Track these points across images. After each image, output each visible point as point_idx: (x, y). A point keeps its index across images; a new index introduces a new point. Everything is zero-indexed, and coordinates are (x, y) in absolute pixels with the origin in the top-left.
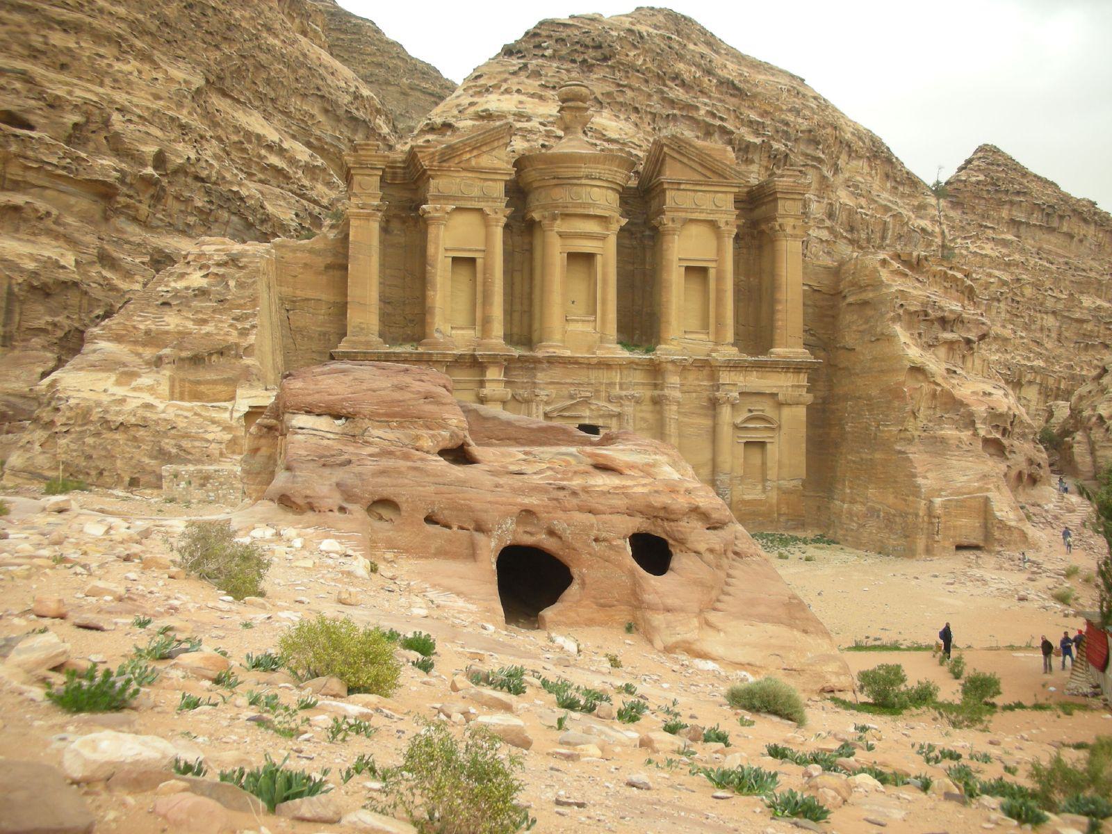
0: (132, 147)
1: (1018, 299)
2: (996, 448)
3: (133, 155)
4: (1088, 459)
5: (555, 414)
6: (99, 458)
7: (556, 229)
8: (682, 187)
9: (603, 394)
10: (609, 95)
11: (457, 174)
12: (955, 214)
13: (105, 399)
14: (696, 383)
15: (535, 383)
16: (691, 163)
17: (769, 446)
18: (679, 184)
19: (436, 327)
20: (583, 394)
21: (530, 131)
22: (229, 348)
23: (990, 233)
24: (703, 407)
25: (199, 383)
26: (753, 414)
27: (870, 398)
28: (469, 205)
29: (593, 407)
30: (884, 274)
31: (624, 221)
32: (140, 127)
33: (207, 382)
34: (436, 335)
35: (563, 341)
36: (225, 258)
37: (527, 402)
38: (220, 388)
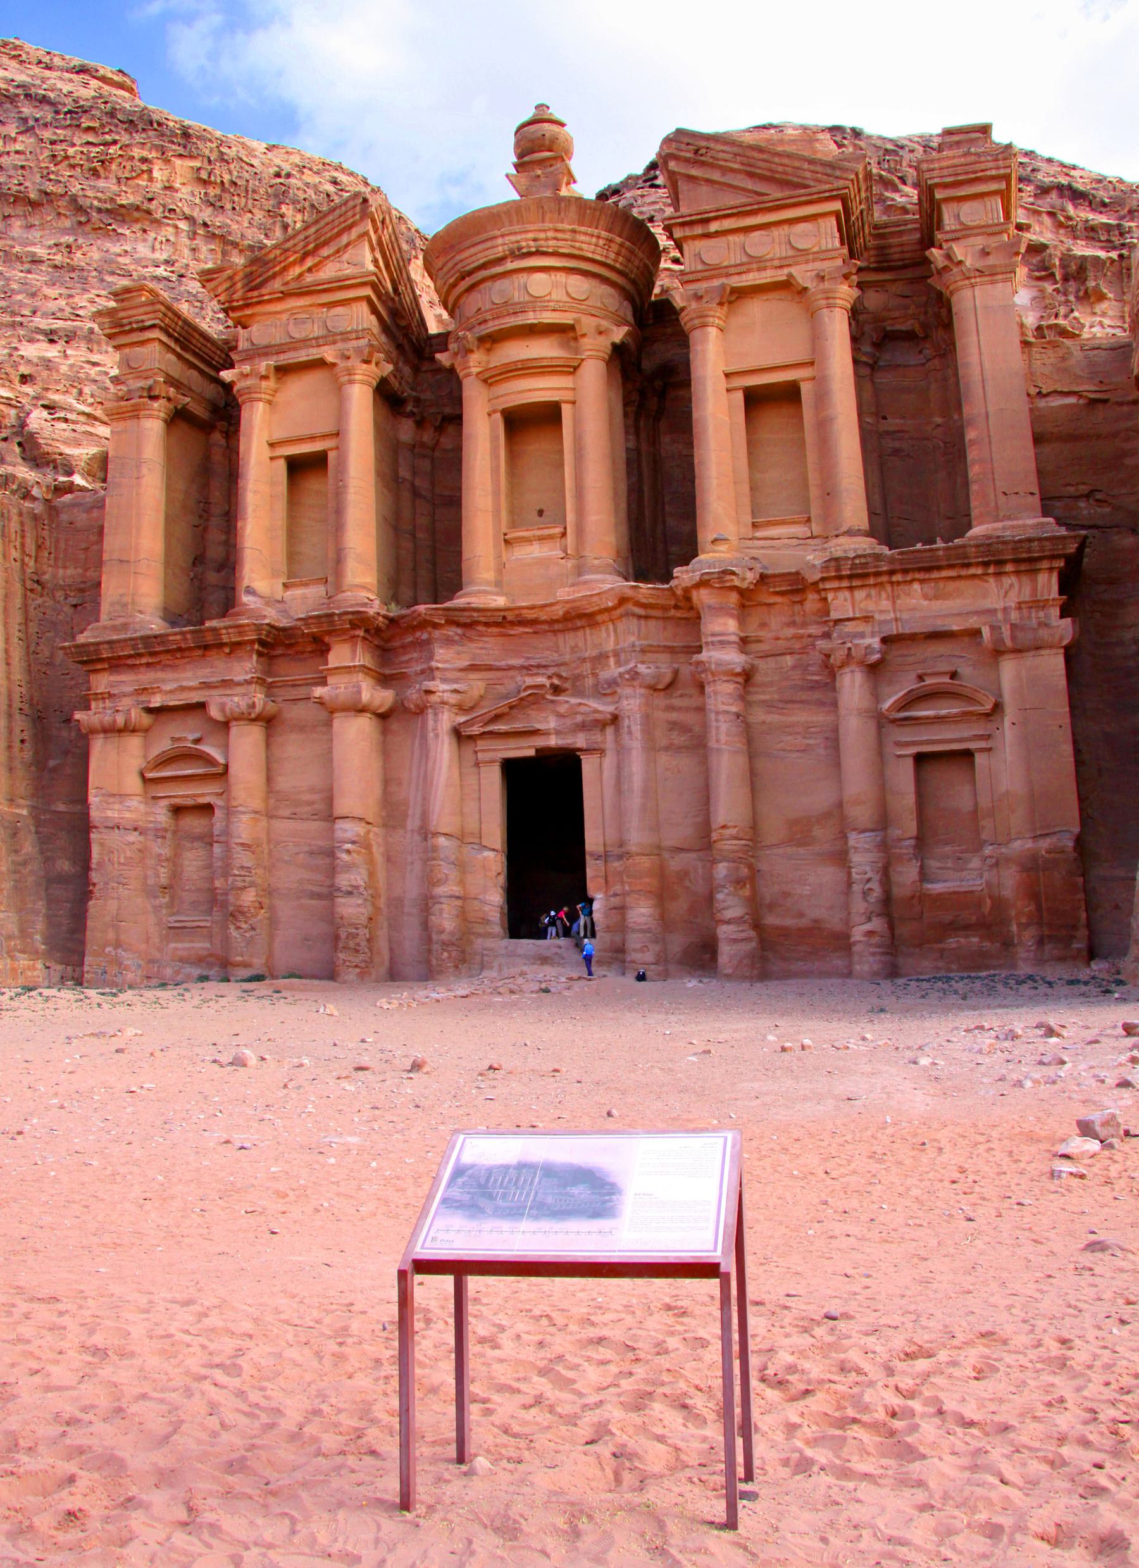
0: (50, 449)
3: (54, 461)
5: (476, 730)
7: (475, 370)
8: (714, 227)
9: (590, 681)
11: (278, 307)
14: (790, 632)
15: (431, 669)
16: (729, 179)
17: (979, 759)
18: (707, 221)
19: (246, 583)
20: (530, 681)
24: (814, 686)
26: (928, 681)
28: (302, 356)
29: (562, 709)
31: (619, 334)
32: (77, 427)
34: (245, 599)
35: (498, 584)
37: (421, 711)
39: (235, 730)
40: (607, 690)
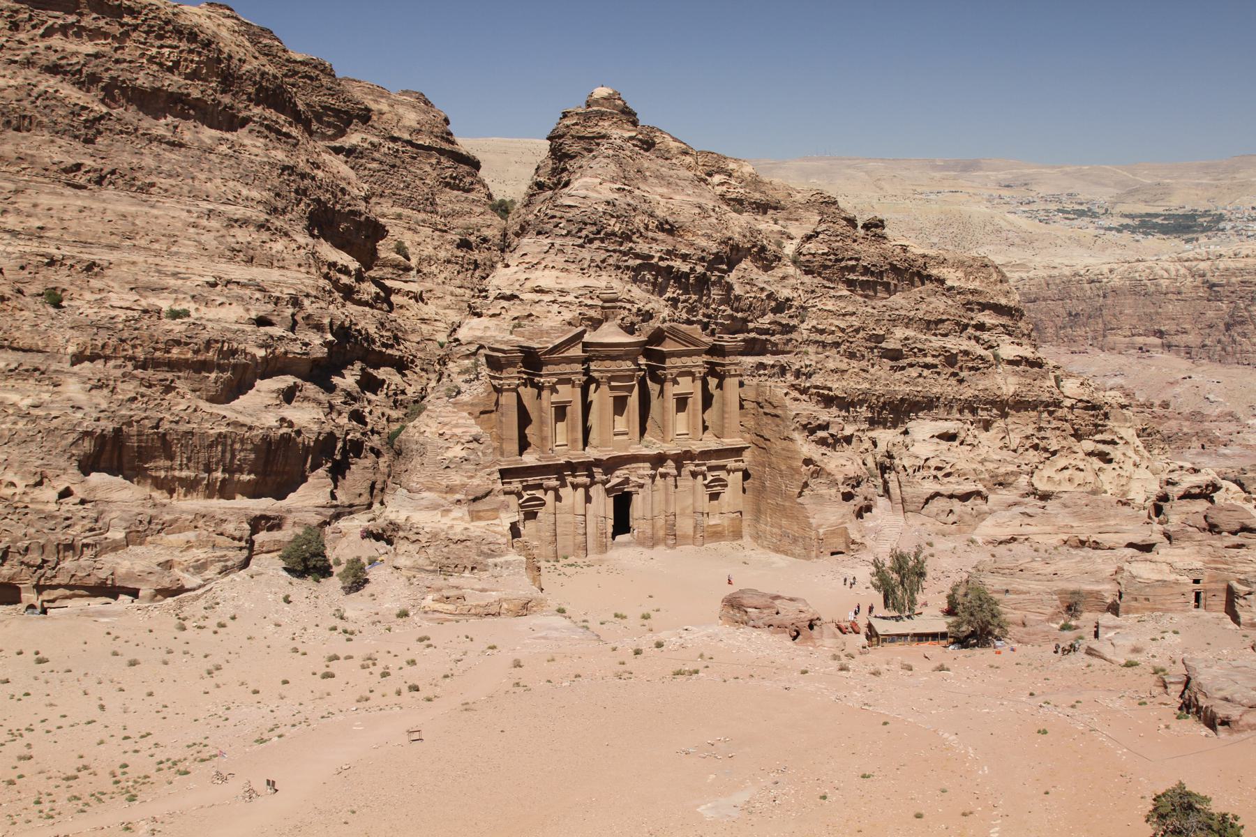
1: (851, 340)
2: (847, 497)
4: (898, 491)
6: (455, 558)
10: (603, 261)
12: (807, 279)
13: (445, 527)
21: (570, 303)
22: (490, 492)
23: (832, 293)
25: (479, 511)
27: (781, 471)
30: (787, 401)
32: (317, 305)
33: (484, 511)
36: (471, 438)
38: (490, 513)
39: (549, 492)
40: (642, 477)
